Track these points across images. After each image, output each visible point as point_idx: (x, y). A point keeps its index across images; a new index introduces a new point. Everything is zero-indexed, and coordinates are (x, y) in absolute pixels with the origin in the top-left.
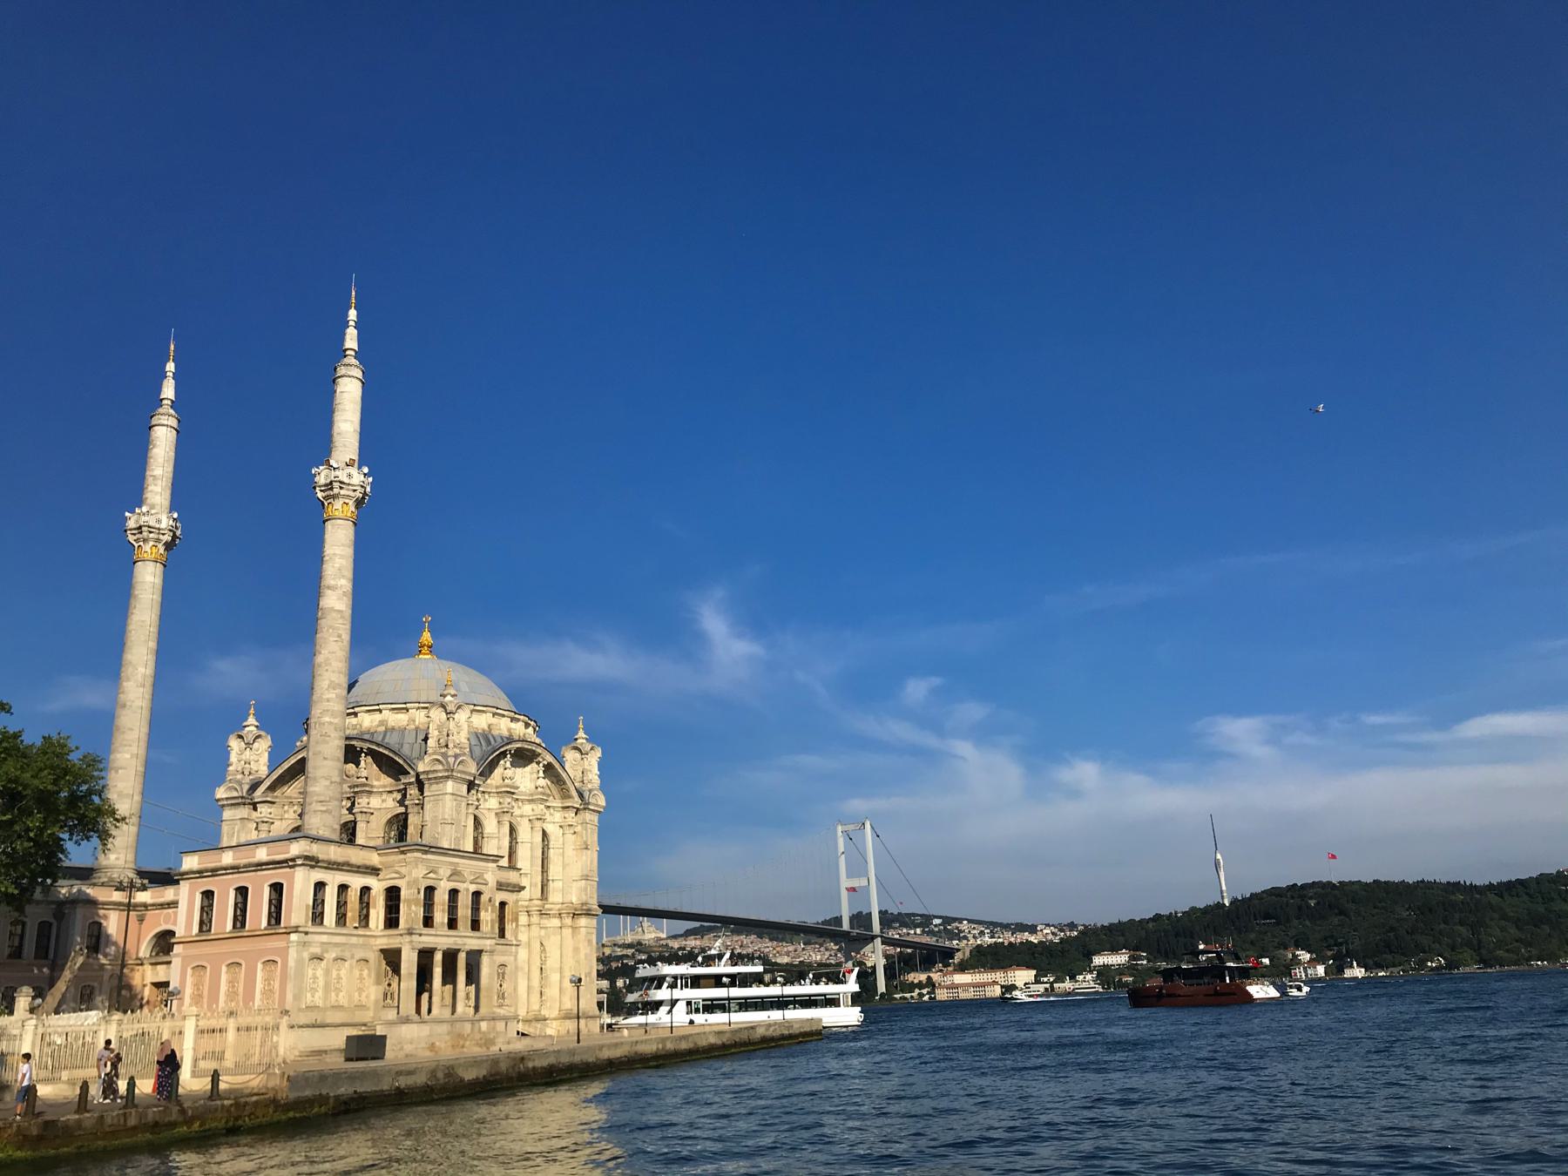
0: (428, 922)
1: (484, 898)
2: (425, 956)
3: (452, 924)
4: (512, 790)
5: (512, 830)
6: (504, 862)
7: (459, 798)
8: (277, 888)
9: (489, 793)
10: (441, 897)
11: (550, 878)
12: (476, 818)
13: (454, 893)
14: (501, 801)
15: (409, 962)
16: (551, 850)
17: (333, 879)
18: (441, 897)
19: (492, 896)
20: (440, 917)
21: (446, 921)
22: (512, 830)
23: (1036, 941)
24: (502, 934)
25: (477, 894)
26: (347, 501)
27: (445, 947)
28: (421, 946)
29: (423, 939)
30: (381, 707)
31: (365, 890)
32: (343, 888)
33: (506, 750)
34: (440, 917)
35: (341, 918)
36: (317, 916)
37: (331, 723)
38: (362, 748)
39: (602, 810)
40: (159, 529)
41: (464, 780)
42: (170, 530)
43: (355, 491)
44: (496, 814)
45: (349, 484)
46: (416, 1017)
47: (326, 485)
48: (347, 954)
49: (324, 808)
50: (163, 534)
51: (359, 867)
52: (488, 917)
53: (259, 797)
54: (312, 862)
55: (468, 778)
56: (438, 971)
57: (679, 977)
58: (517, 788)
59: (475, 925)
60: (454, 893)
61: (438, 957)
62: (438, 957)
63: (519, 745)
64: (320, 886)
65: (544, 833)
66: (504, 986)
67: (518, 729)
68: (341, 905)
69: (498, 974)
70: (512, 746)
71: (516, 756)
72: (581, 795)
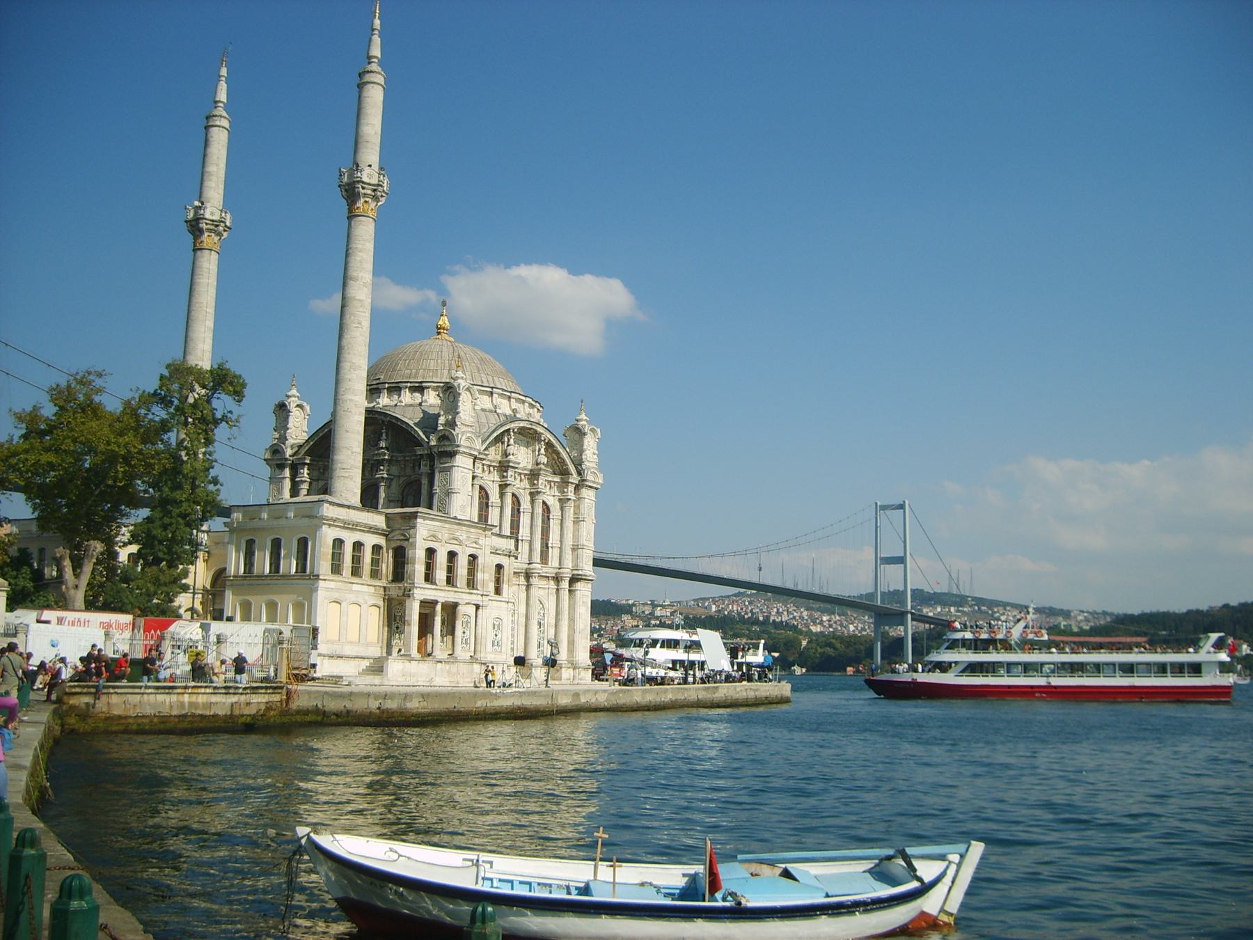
0: (429, 578)
1: (480, 560)
2: (428, 605)
3: (450, 581)
4: (516, 466)
5: (516, 500)
6: (507, 531)
7: (466, 470)
8: (303, 543)
9: (494, 467)
10: (441, 559)
11: (550, 545)
12: (481, 488)
13: (452, 555)
14: (505, 474)
15: (414, 612)
16: (551, 520)
17: (350, 538)
18: (441, 559)
19: (487, 562)
20: (441, 574)
21: (445, 578)
22: (516, 500)
23: (814, 631)
24: (498, 591)
25: (473, 558)
26: (367, 199)
27: (441, 600)
28: (422, 598)
29: (427, 592)
30: (401, 385)
31: (376, 549)
32: (358, 546)
33: (509, 429)
34: (441, 574)
35: (356, 572)
36: (336, 569)
37: (350, 400)
38: (383, 421)
39: (599, 487)
40: (213, 221)
41: (471, 455)
42: (222, 222)
43: (374, 190)
44: (500, 485)
45: (369, 184)
46: (418, 656)
47: (348, 184)
48: (361, 601)
49: (347, 475)
50: (217, 226)
51: (371, 528)
52: (485, 577)
53: (299, 459)
54: (333, 522)
55: (472, 452)
56: (438, 620)
57: (660, 642)
58: (519, 463)
59: (471, 583)
60: (452, 555)
61: (439, 608)
62: (439, 608)
63: (522, 425)
64: (338, 543)
65: (544, 503)
66: (499, 636)
67: (523, 411)
68: (357, 560)
69: (494, 625)
70: (512, 425)
71: (519, 433)
72: (579, 474)
